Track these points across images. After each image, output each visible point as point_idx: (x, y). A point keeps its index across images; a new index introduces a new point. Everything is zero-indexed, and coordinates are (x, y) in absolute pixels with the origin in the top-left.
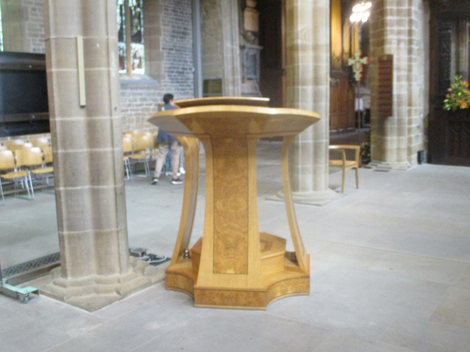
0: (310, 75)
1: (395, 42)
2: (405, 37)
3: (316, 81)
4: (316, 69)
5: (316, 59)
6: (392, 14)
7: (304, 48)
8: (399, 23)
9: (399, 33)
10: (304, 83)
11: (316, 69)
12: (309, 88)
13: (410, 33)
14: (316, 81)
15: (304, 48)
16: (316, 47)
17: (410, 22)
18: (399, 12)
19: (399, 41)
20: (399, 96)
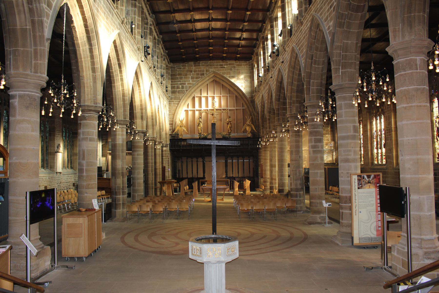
0: (159, 174)
1: (165, 163)
2: (167, 162)
3: (160, 175)
4: (160, 173)
5: (160, 171)
6: (164, 157)
7: (158, 169)
8: (166, 159)
9: (166, 161)
10: (158, 175)
11: (160, 173)
12: (159, 176)
13: (168, 161)
14: (160, 175)
15: (158, 169)
16: (160, 169)
17: (168, 158)
18: (166, 156)
19: (166, 163)
20: (166, 176)
